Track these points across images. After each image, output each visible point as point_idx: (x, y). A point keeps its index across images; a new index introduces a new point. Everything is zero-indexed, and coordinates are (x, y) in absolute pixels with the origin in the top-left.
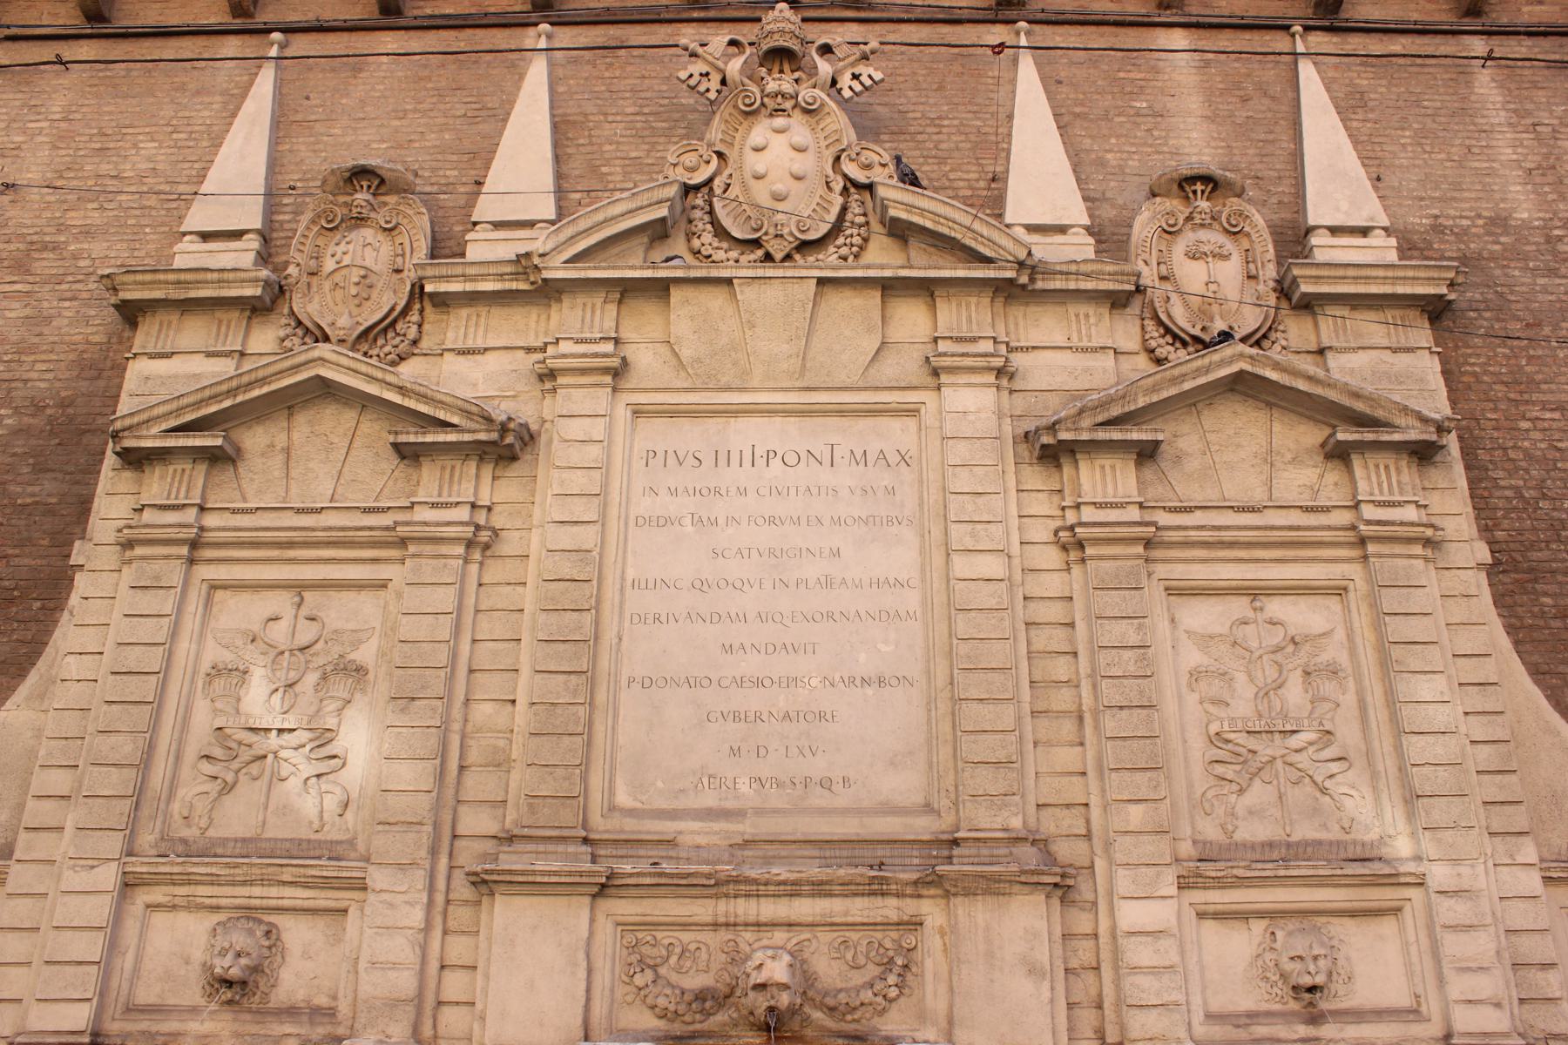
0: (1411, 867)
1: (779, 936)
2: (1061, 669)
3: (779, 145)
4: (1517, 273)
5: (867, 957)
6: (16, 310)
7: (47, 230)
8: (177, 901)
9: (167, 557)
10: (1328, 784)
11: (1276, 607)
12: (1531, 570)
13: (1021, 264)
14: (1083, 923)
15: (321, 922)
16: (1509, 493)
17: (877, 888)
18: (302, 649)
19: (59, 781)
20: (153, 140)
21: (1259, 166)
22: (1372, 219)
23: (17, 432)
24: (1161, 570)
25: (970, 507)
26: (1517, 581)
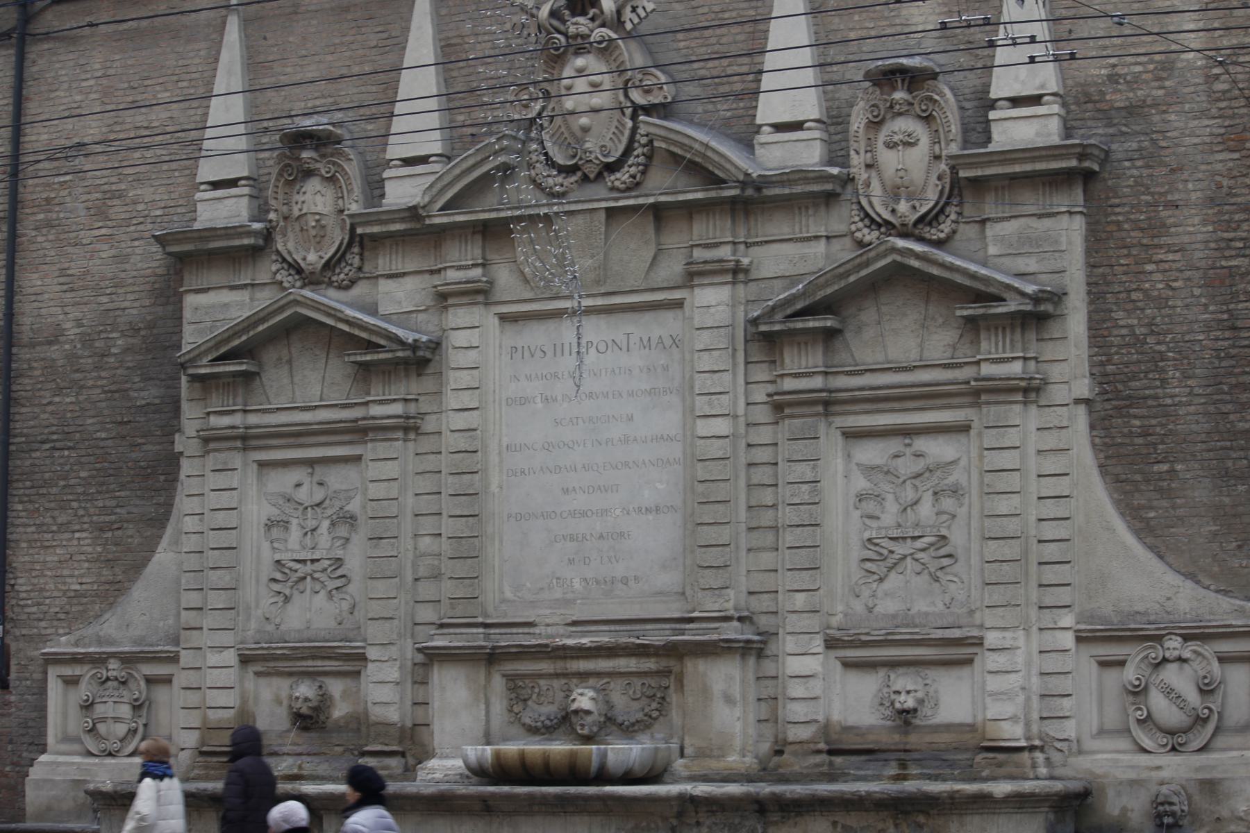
0: (975, 633)
2: (768, 497)
4: (1173, 117)
5: (643, 694)
7: (113, 179)
9: (229, 449)
10: (939, 574)
11: (921, 444)
12: (1129, 397)
13: (743, 185)
16: (1124, 331)
18: (318, 505)
20: (166, 90)
22: (1042, 86)
23: (126, 350)
24: (839, 421)
26: (1116, 408)
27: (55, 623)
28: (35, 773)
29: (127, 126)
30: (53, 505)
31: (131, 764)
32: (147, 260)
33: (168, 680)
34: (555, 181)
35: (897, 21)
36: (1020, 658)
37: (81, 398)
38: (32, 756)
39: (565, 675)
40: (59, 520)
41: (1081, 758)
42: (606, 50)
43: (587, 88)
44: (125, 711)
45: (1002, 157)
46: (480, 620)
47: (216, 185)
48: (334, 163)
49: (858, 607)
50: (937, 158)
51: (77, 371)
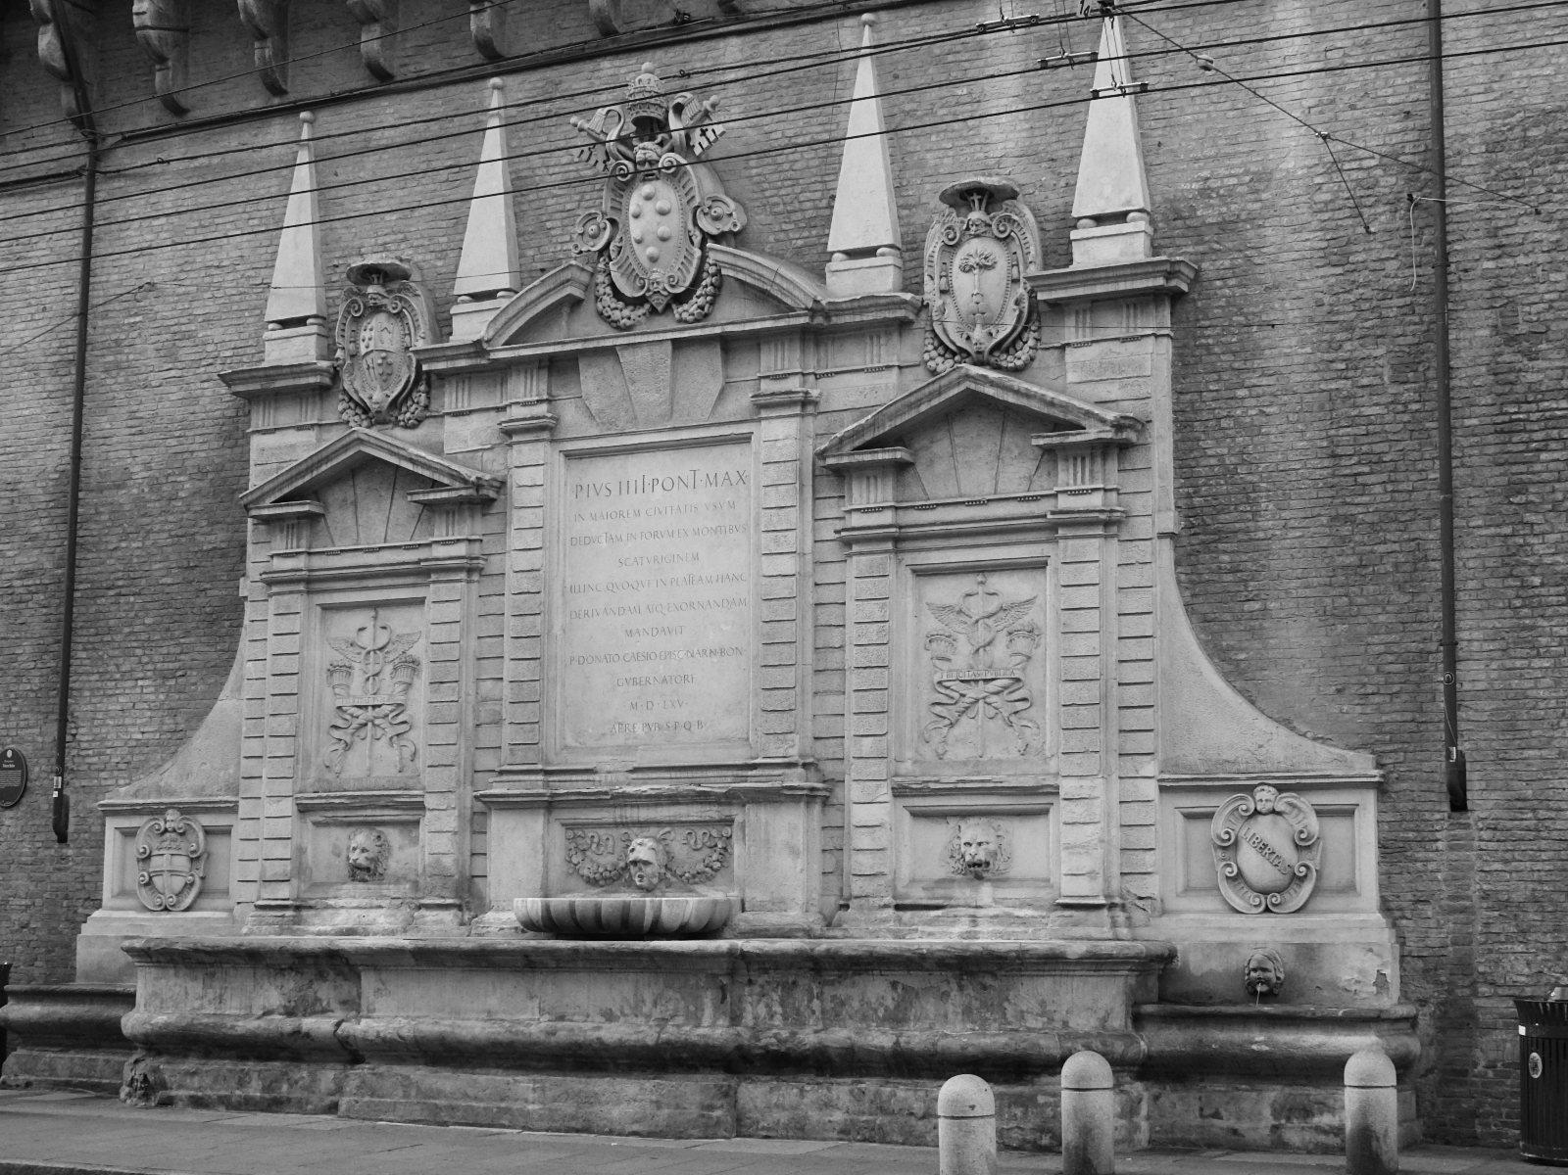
0: (1050, 781)
1: (653, 830)
3: (649, 208)
4: (1269, 232)
6: (175, 393)
7: (183, 320)
9: (291, 592)
12: (1218, 532)
13: (813, 312)
14: (834, 817)
16: (1213, 461)
17: (703, 798)
18: (381, 649)
21: (1055, 146)
22: (1129, 203)
24: (909, 558)
25: (775, 519)
26: (1203, 542)
27: (116, 773)
28: (87, 929)
29: (198, 266)
30: (117, 653)
31: (186, 919)
32: (214, 399)
33: (226, 832)
34: (622, 314)
35: (977, 141)
36: (1098, 808)
37: (148, 543)
38: (87, 912)
39: (624, 824)
40: (123, 669)
41: (1164, 919)
42: (676, 174)
43: (653, 217)
44: (182, 863)
45: (1085, 277)
46: (540, 767)
47: (285, 324)
48: (401, 299)
49: (928, 753)
50: (1016, 281)
51: (144, 516)
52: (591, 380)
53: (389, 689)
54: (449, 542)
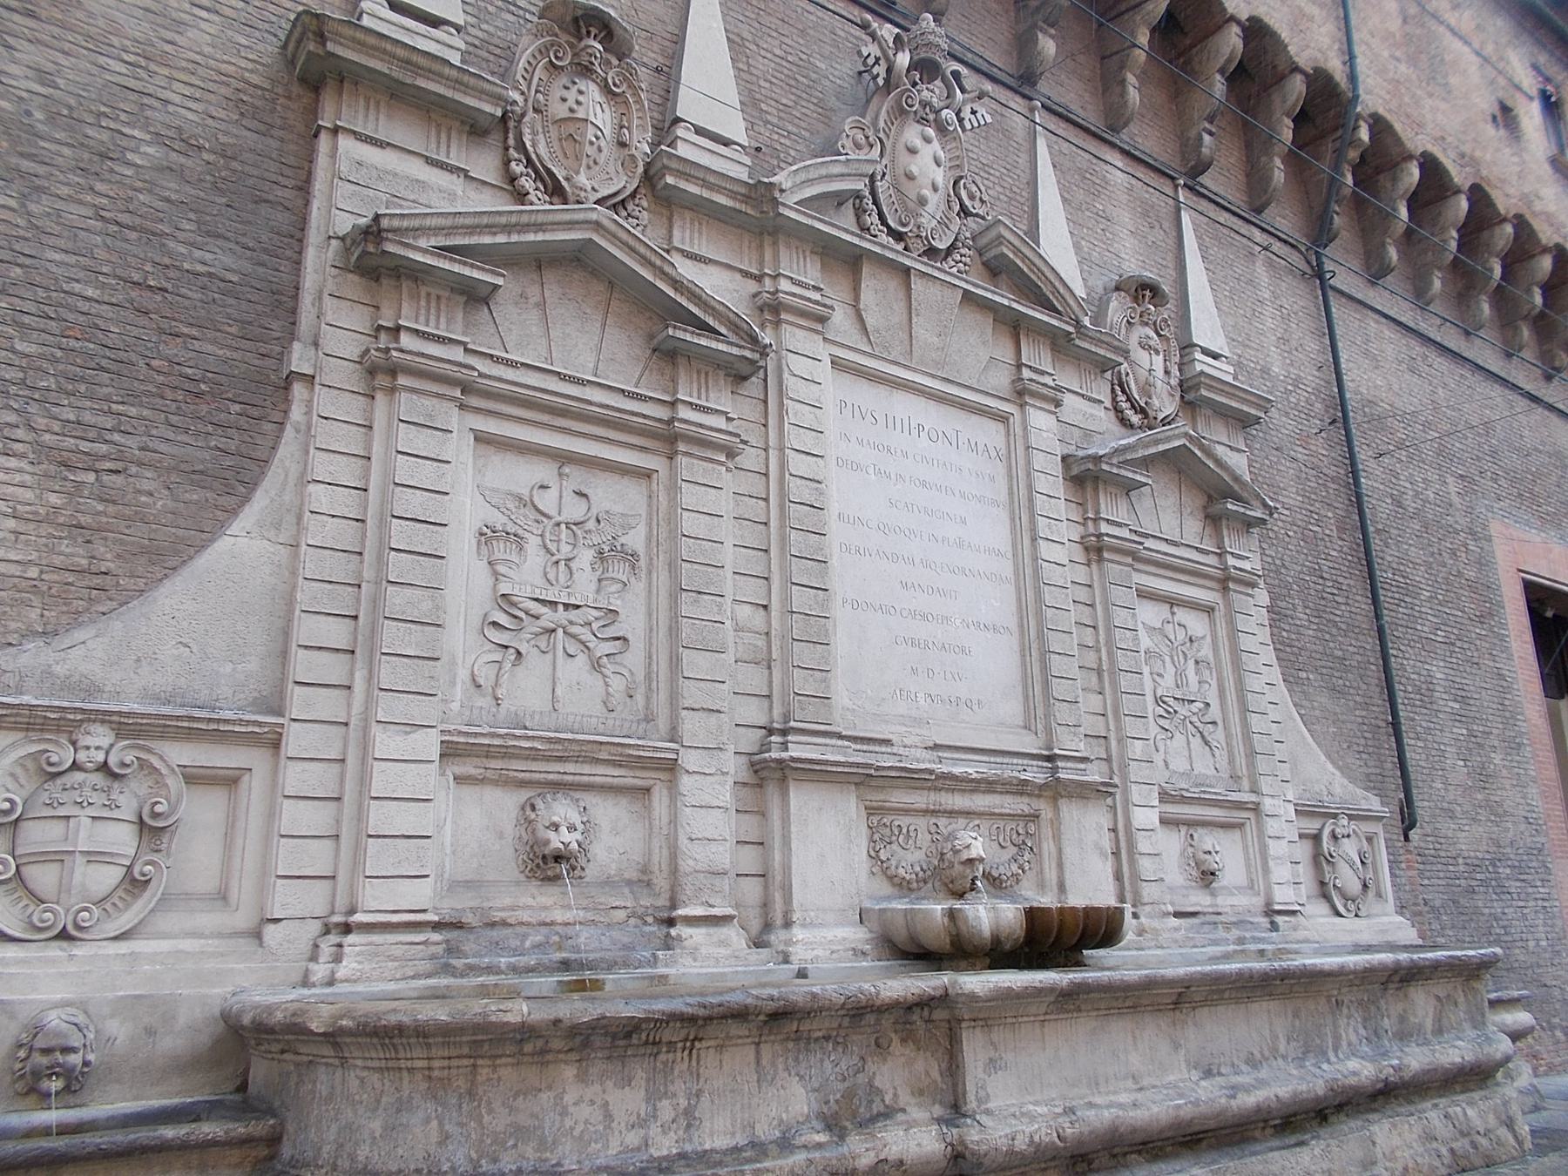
0: (1253, 798)
8: (489, 774)
9: (438, 396)
11: (1182, 615)
15: (624, 801)
19: (336, 632)
44: (121, 839)
51: (30, 157)
52: (875, 290)
53: (584, 586)
54: (714, 408)
